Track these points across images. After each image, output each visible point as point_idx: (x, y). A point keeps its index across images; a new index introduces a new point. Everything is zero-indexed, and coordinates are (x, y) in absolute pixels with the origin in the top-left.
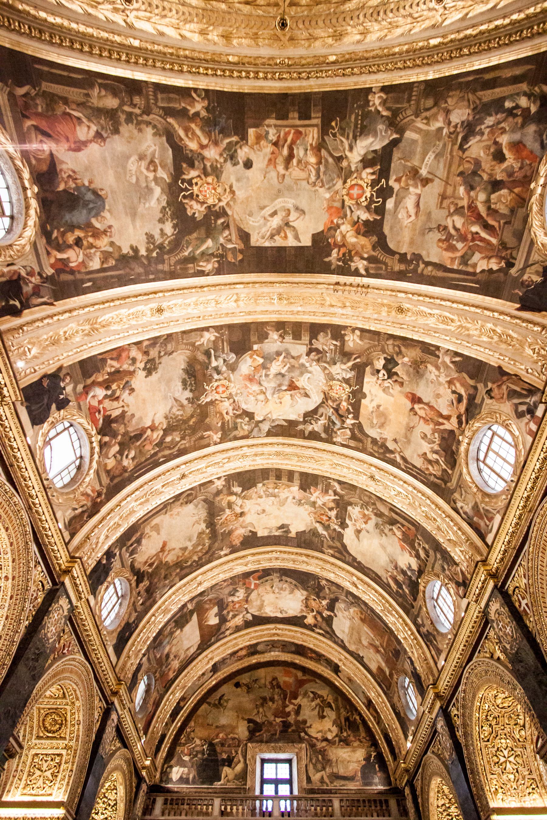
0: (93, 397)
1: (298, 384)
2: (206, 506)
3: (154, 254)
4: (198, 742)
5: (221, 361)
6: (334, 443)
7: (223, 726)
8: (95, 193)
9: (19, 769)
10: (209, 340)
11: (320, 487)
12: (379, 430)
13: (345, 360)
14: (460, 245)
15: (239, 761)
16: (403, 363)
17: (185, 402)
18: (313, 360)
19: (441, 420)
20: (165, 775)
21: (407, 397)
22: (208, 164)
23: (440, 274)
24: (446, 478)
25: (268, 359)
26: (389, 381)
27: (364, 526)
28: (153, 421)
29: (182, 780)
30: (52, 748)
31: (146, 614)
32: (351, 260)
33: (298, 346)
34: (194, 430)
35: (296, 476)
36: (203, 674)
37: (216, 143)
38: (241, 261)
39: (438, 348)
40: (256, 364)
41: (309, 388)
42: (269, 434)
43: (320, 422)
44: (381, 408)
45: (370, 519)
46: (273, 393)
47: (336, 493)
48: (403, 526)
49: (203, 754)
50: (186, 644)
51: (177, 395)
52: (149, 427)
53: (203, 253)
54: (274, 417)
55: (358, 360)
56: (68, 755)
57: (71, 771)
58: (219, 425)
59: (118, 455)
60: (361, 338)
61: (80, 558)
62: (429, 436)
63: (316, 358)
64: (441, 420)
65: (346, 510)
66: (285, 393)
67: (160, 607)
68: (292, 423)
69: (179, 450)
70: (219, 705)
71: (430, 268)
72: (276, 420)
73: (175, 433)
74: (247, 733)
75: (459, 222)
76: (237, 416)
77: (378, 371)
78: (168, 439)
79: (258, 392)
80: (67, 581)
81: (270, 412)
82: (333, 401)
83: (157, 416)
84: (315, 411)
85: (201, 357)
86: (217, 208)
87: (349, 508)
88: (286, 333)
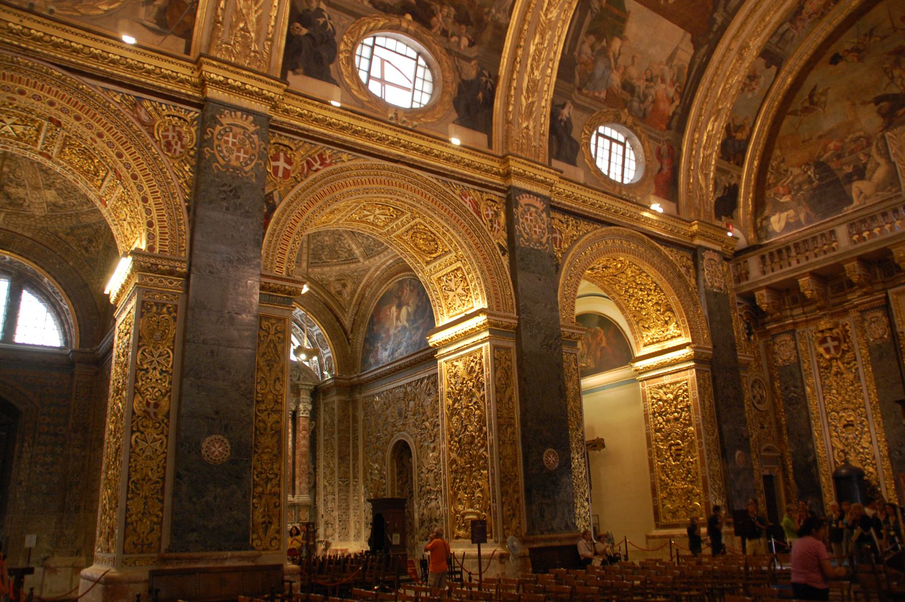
4: (796, 171)
7: (831, 131)
9: (434, 298)
15: (878, 165)
20: (761, 229)
29: (788, 226)
30: (446, 266)
31: (500, 51)
36: (752, 77)
49: (811, 182)
50: (659, 54)
56: (464, 265)
57: (478, 278)
61: (201, 55)
67: (520, 31)
70: (813, 103)
74: (879, 121)
80: (213, 93)
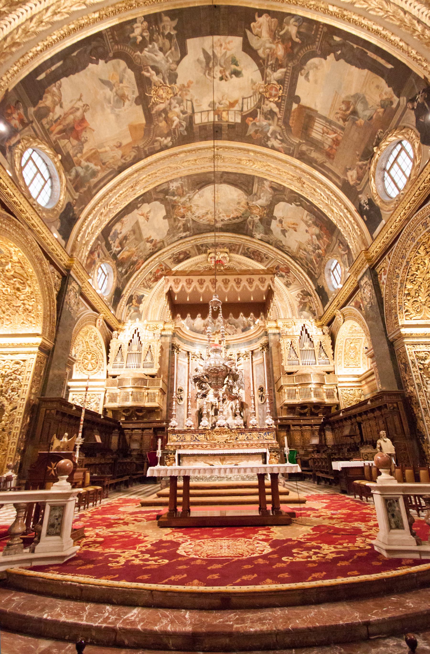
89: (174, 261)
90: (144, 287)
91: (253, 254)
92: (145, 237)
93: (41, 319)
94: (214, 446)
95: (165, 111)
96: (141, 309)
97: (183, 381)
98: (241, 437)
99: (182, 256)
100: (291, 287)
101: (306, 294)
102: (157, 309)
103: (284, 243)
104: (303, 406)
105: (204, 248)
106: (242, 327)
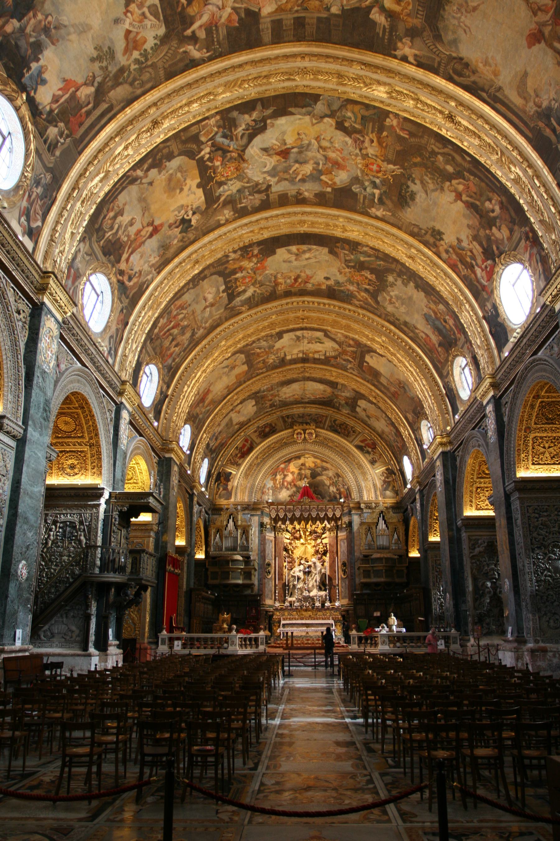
0: (483, 277)
1: (278, 158)
2: (441, 25)
3: (405, 277)
5: (368, 189)
6: (217, 113)
8: (427, 320)
10: (378, 210)
11: (223, 32)
12: (171, 172)
13: (229, 198)
14: (175, 313)
16: (176, 237)
17: (417, 182)
18: (263, 183)
19: (130, 250)
21: (162, 225)
22: (355, 285)
23: (178, 296)
24: (100, 234)
25: (315, 176)
26: (181, 217)
27: (127, 26)
28: (455, 201)
32: (242, 255)
33: (282, 189)
34: (419, 150)
35: (267, 36)
37: (348, 290)
38: (336, 242)
39: (159, 273)
40: (327, 176)
41: (265, 158)
42: (316, 98)
43: (244, 126)
44: (178, 191)
45: (127, 51)
46: (309, 144)
47: (194, 39)
48: (88, 113)
51: (424, 195)
52: (461, 200)
53: (369, 256)
54: (307, 118)
55: (215, 206)
58: (385, 134)
59: (498, 225)
60: (219, 221)
62: (130, 228)
63: (260, 187)
64: (130, 250)
65: (167, 22)
66: (294, 145)
68: (282, 112)
69: (445, 146)
71: (185, 290)
72: (305, 115)
73: (442, 167)
75: (181, 316)
76: (359, 132)
77: (194, 213)
78: (450, 168)
79: (328, 150)
81: (313, 125)
82: (231, 158)
83: (449, 199)
84: (251, 137)
85: (388, 202)
86: (352, 269)
87: (162, 31)
88: (296, 197)
89: (260, 434)
90: (232, 463)
91: (340, 428)
92: (234, 423)
93: (184, 533)
94: (302, 619)
95: (264, 360)
96: (229, 487)
97: (270, 555)
98: (319, 613)
99: (267, 430)
100: (377, 465)
101: (390, 472)
102: (246, 488)
103: (369, 423)
104: (377, 584)
105: (290, 420)
106: (328, 498)
